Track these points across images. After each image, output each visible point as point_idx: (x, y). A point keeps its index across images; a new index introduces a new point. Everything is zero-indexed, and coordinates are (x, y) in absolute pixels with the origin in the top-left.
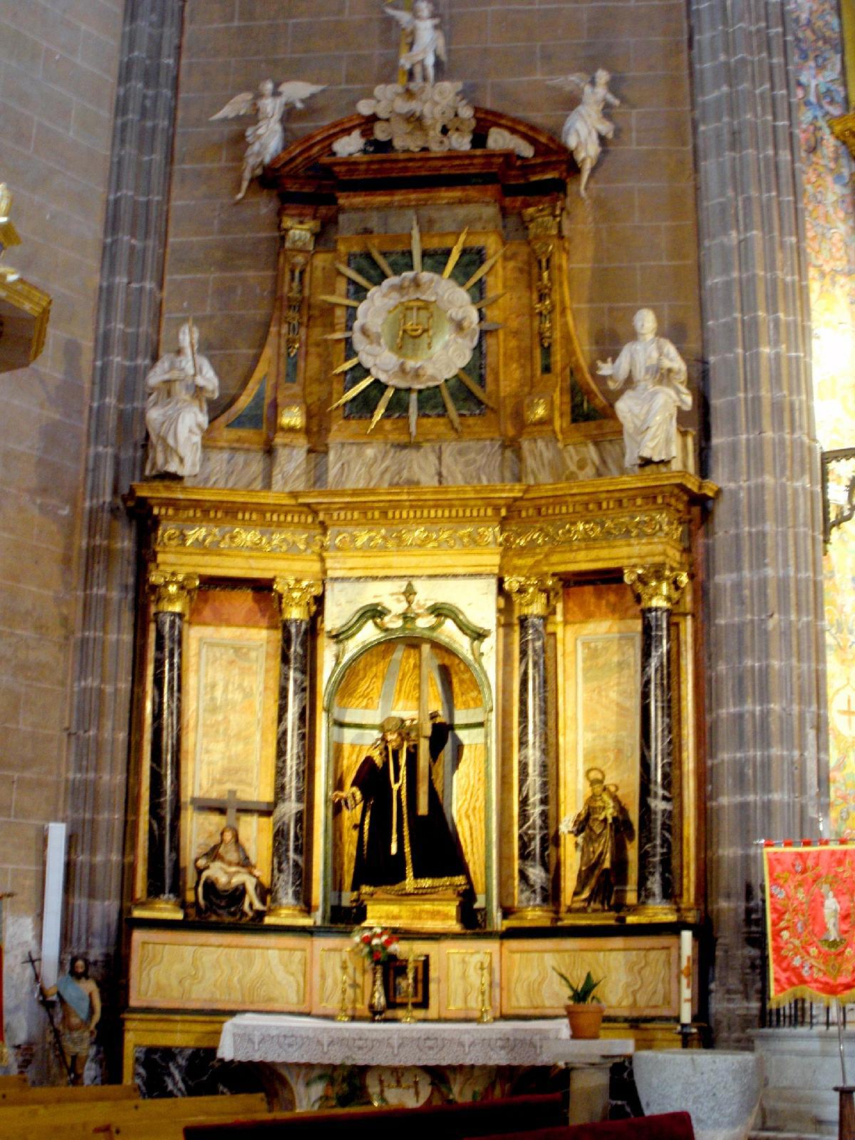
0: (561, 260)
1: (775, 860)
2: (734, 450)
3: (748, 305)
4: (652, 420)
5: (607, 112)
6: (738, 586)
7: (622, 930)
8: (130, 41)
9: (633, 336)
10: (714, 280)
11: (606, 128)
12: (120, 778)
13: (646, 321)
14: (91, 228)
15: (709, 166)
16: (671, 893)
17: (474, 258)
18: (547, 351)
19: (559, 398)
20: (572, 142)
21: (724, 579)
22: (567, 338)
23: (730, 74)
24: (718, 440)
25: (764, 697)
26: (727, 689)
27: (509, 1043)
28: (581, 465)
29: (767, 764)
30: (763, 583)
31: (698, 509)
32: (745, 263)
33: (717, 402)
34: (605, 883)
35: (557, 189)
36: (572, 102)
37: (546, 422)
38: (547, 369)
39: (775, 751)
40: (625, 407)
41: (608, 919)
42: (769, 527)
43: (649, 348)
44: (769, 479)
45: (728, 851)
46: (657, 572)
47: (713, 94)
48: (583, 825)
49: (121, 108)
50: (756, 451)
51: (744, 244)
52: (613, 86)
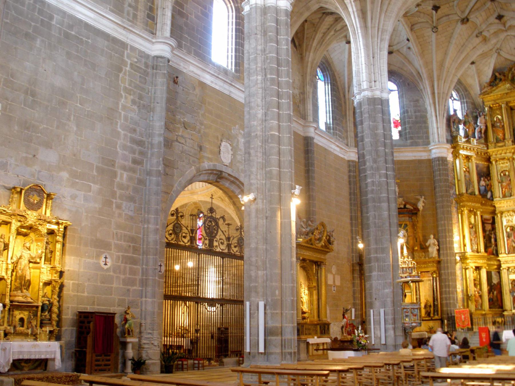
0: (418, 225)
1: (456, 312)
2: (443, 254)
3: (445, 233)
4: (433, 251)
5: (424, 202)
6: (445, 273)
7: (432, 320)
8: (350, 188)
9: (430, 238)
10: (440, 228)
11: (423, 204)
12: (360, 302)
13: (432, 236)
14: (348, 220)
15: (439, 211)
16: (438, 315)
17: (406, 225)
18: (416, 239)
19: (419, 246)
20: (419, 208)
21: (443, 272)
22: (419, 237)
23: (442, 197)
24: (441, 252)
25: (449, 288)
26: (444, 287)
27: (419, 335)
28: (422, 255)
29: (450, 297)
30: (448, 273)
31: (439, 262)
32: (445, 226)
33: (441, 246)
34: (428, 314)
35: (416, 214)
36: (418, 200)
37: (417, 250)
38: (416, 241)
39: (451, 295)
40: (430, 249)
41: (430, 318)
42: (449, 265)
43: (432, 241)
44: (449, 258)
45: (445, 309)
46: (435, 272)
47: (439, 199)
48: (425, 307)
49: (350, 199)
50: (447, 254)
51: (444, 223)
52: (425, 199)
